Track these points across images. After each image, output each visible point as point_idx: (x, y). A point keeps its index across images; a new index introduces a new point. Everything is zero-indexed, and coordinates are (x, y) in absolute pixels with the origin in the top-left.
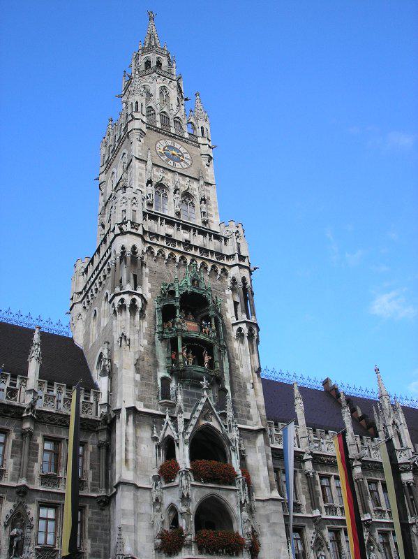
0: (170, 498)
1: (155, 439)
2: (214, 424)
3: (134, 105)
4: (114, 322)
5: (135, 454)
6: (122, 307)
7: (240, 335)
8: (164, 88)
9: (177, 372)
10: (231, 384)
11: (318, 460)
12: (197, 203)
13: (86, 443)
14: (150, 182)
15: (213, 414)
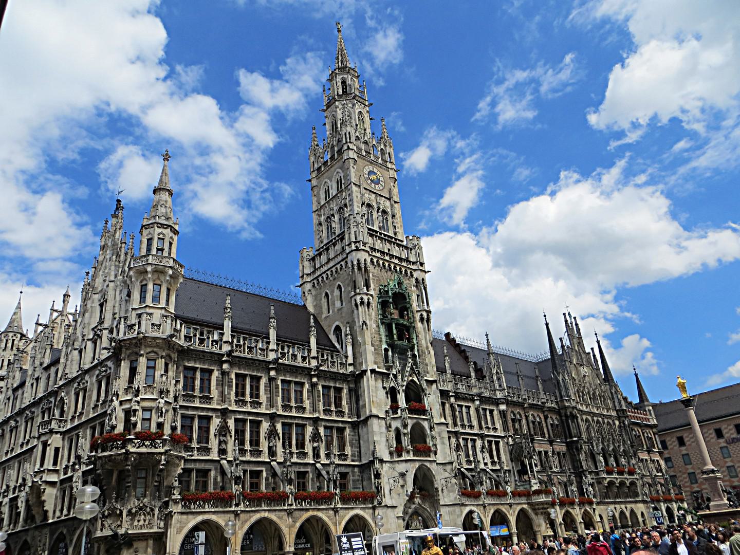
0: (396, 424)
1: (384, 388)
2: (415, 379)
3: (348, 136)
4: (356, 311)
5: (375, 396)
6: (362, 303)
7: (422, 319)
8: (360, 113)
9: (391, 345)
10: (418, 350)
11: (458, 396)
12: (390, 218)
13: (343, 388)
14: (363, 204)
15: (415, 373)
